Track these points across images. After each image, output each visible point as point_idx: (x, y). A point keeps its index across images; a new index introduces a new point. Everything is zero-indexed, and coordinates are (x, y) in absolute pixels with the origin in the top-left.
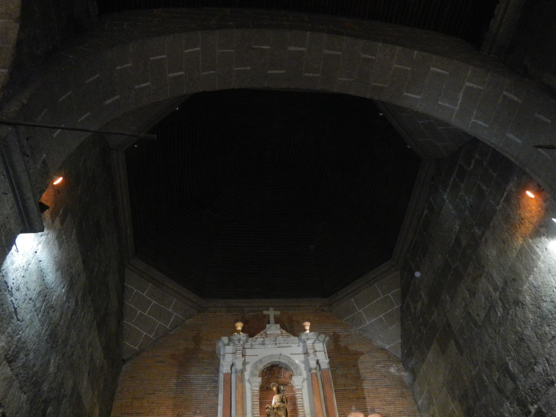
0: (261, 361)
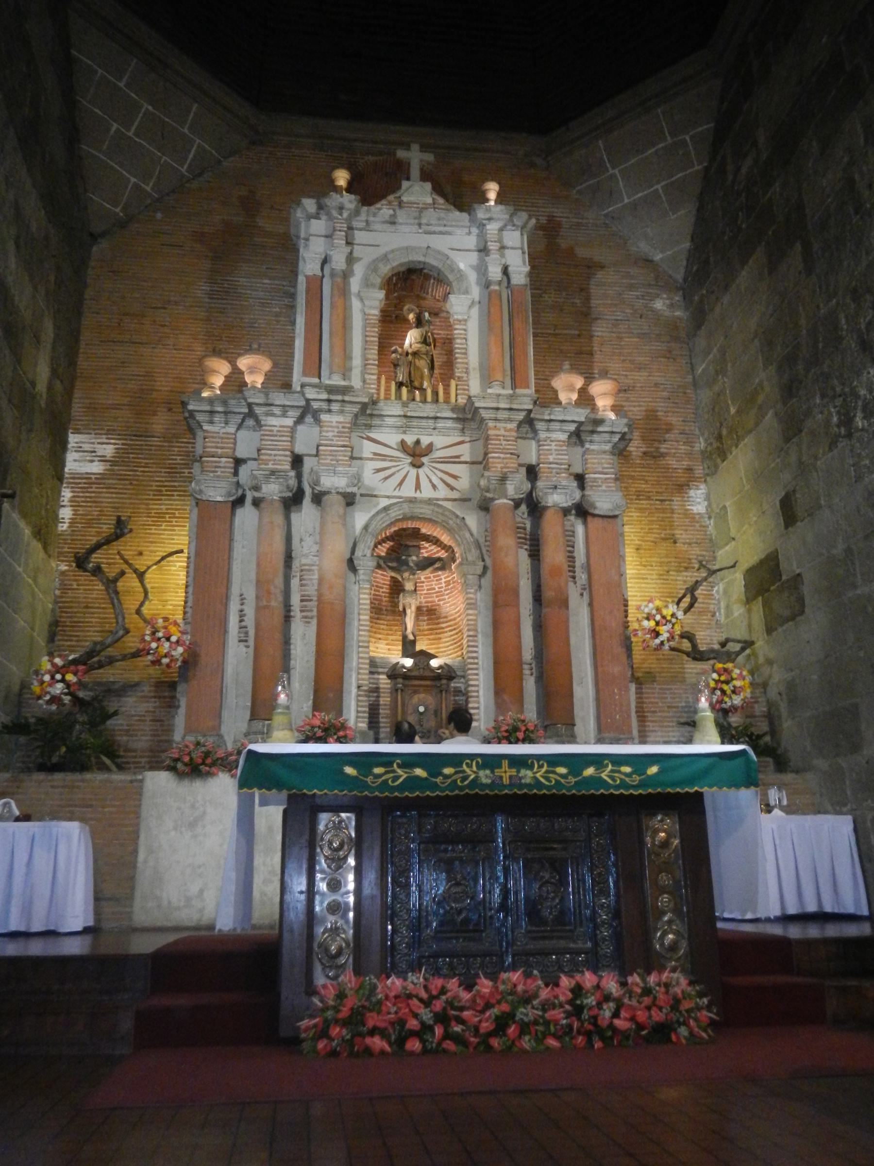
0: (385, 258)
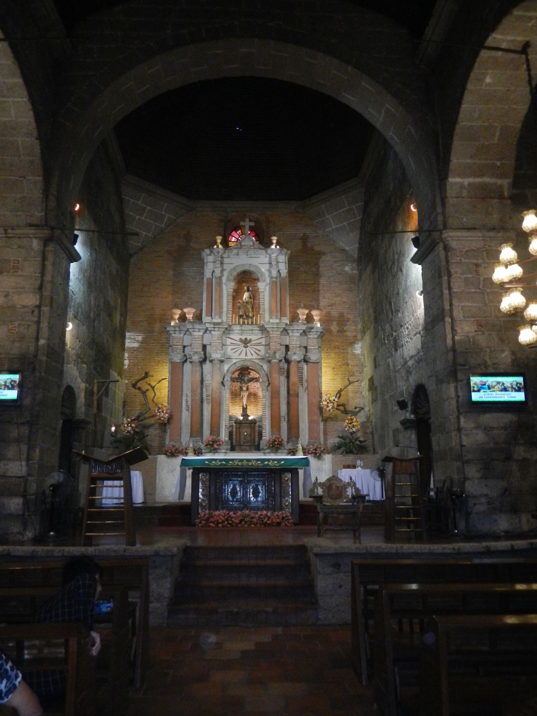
0: (235, 269)
